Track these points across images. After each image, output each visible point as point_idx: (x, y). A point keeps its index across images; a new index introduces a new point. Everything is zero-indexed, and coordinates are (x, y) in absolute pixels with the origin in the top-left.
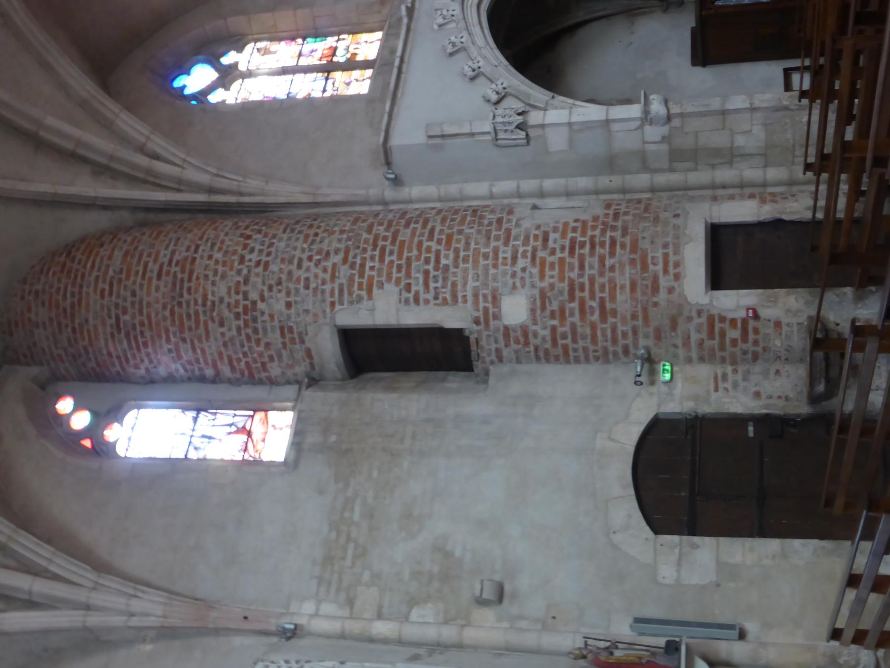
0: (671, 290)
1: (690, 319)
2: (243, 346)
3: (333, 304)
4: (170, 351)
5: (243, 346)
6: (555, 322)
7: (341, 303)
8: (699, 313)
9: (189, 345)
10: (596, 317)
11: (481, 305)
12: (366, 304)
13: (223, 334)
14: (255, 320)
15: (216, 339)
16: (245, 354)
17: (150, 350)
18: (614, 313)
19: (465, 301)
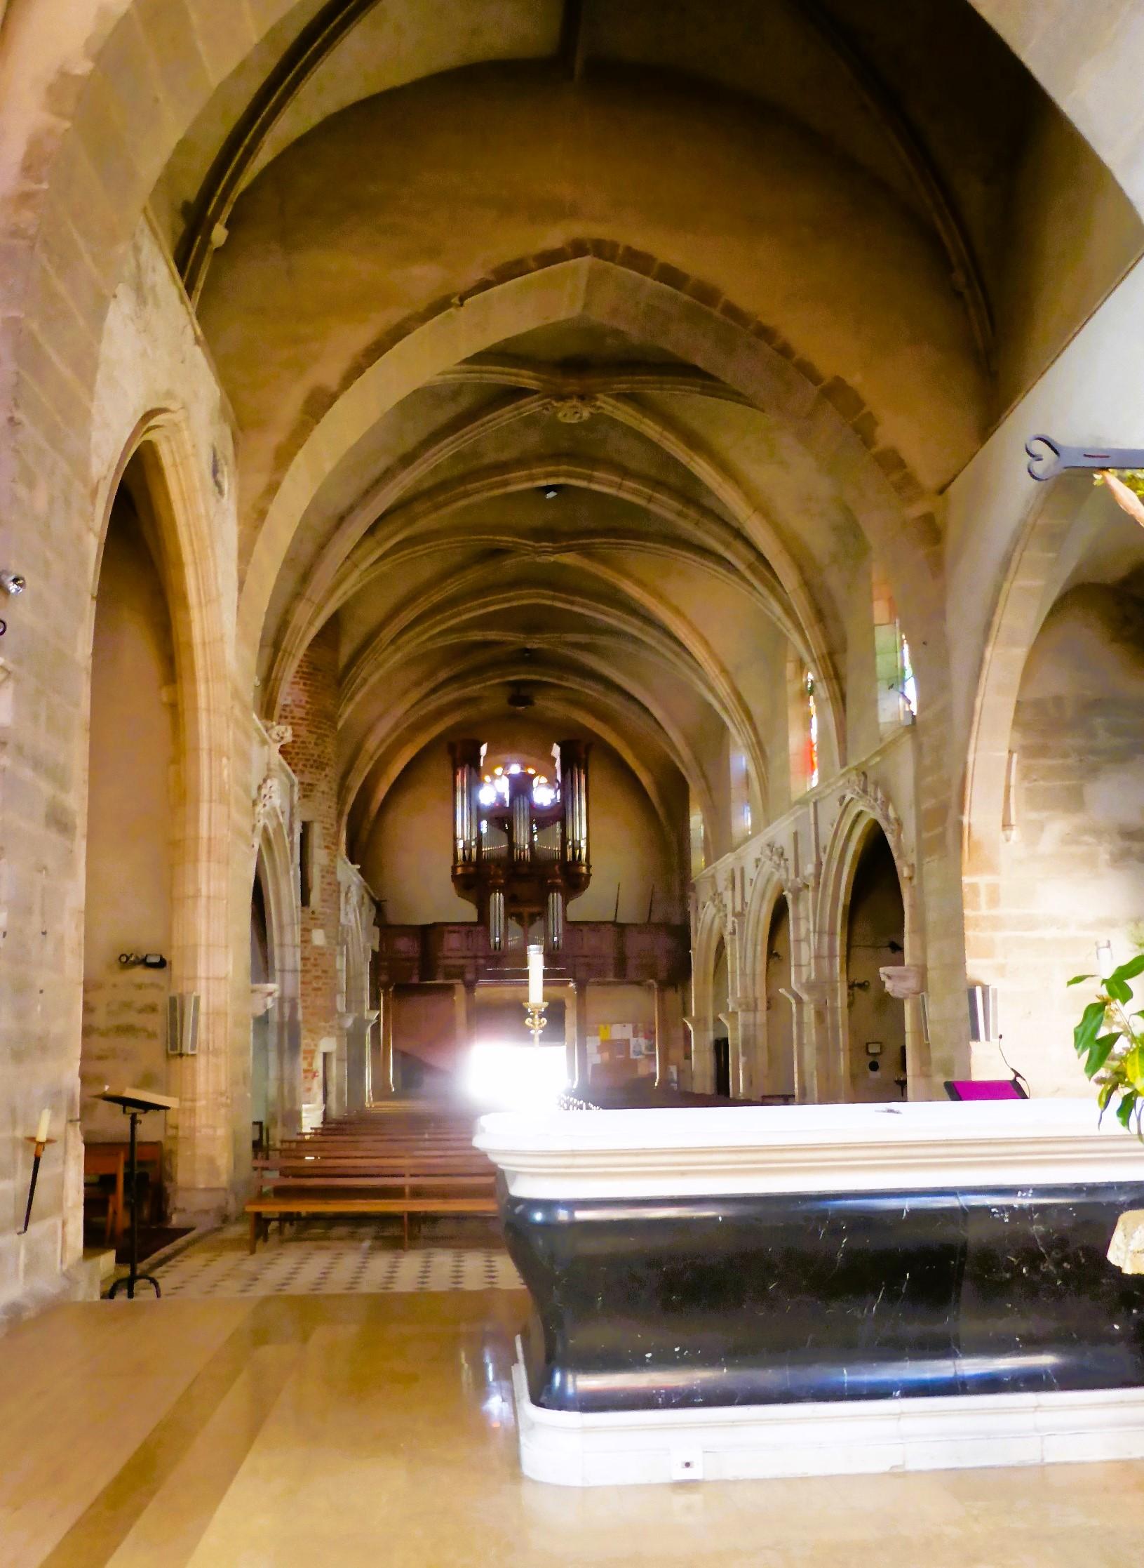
0: (325, 1028)
1: (313, 1040)
2: (303, 754)
3: (323, 822)
4: (301, 701)
5: (303, 754)
6: (312, 960)
7: (324, 828)
8: (316, 1045)
9: (304, 716)
10: (315, 985)
11: (322, 917)
12: (323, 844)
13: (310, 743)
14: (317, 768)
15: (308, 737)
16: (297, 754)
17: (301, 686)
18: (316, 996)
19: (323, 907)
